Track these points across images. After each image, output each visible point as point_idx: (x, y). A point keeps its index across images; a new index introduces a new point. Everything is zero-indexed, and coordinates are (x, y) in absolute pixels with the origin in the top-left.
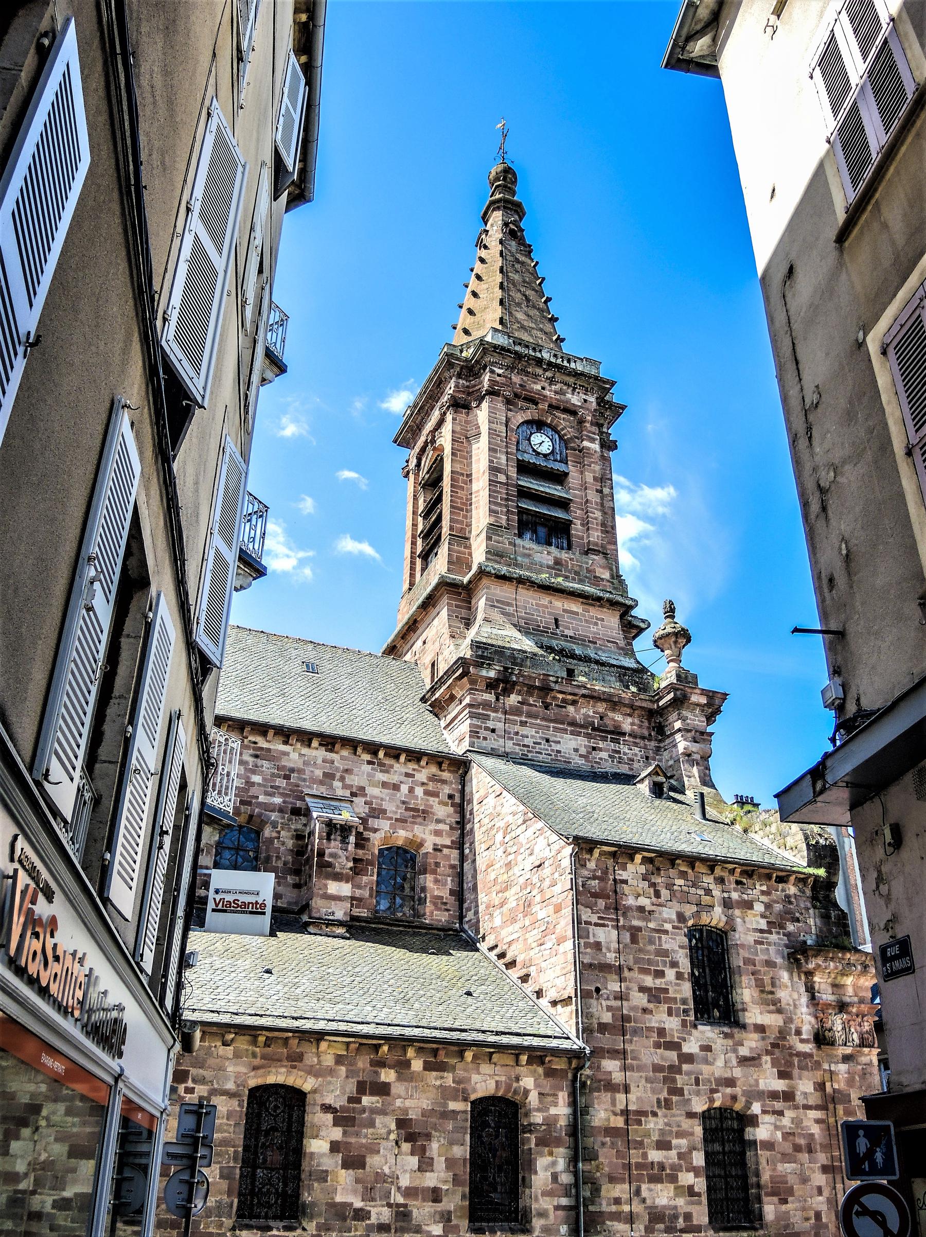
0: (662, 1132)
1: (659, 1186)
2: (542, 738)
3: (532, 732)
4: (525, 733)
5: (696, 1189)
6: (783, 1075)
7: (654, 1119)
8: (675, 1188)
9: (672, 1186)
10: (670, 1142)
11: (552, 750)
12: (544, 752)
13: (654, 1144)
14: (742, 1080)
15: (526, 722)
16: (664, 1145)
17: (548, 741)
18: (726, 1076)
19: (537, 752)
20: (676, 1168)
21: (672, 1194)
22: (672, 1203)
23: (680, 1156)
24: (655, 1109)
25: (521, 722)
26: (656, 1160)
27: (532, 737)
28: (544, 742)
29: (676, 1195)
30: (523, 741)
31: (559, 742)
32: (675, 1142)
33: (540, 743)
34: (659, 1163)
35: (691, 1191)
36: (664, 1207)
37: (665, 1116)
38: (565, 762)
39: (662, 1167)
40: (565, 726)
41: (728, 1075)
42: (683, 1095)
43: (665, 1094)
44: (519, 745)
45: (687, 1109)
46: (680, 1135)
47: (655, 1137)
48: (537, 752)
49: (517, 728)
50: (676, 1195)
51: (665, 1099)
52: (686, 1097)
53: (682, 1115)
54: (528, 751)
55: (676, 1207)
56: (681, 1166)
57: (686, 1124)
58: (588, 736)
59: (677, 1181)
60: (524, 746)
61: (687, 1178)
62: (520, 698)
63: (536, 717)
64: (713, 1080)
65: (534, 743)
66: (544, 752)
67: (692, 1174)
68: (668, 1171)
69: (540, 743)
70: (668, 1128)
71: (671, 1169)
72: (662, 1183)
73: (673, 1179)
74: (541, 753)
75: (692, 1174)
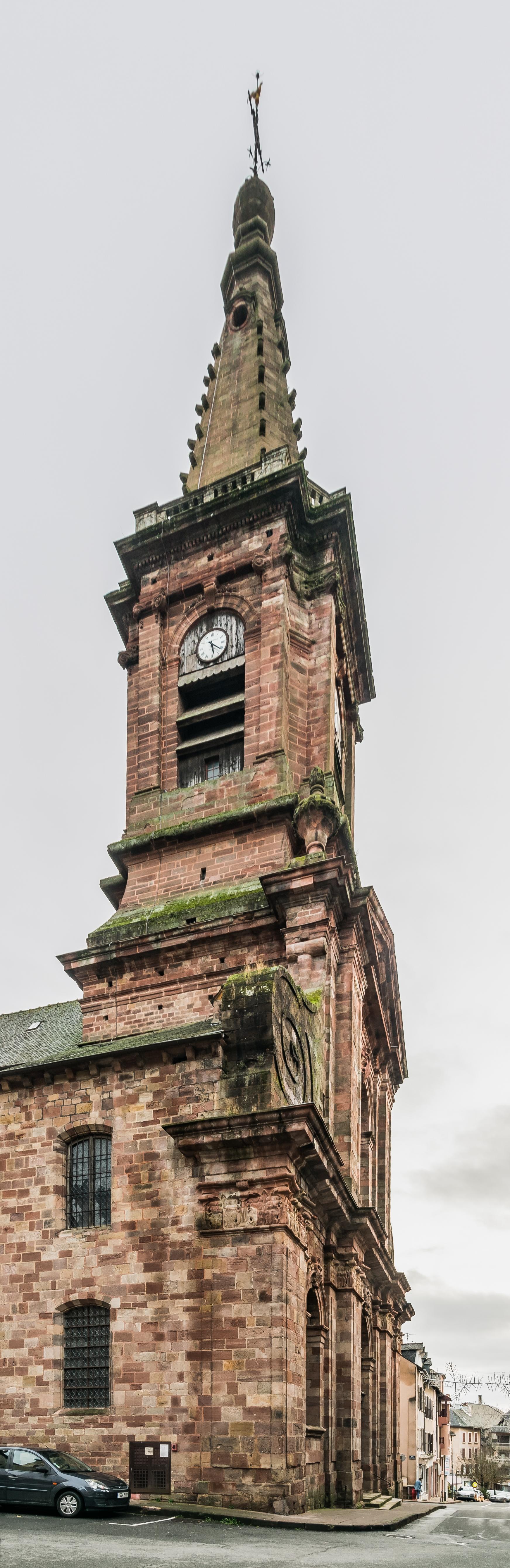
0: (15, 1334)
1: (10, 1378)
2: (153, 1007)
3: (145, 1005)
4: (137, 1008)
5: (44, 1379)
6: (148, 1268)
7: (9, 1322)
8: (24, 1379)
9: (21, 1378)
10: (23, 1341)
11: (165, 1016)
12: (155, 1021)
13: (7, 1344)
14: (102, 1278)
15: (137, 997)
16: (16, 1344)
17: (160, 1007)
18: (85, 1276)
19: (149, 1024)
20: (26, 1363)
21: (21, 1384)
22: (21, 1391)
23: (31, 1352)
24: (11, 1314)
25: (132, 999)
26: (8, 1357)
27: (144, 1009)
28: (157, 1010)
29: (25, 1385)
30: (134, 1017)
31: (172, 1004)
32: (27, 1340)
33: (152, 1013)
34: (10, 1359)
35: (40, 1381)
36: (13, 1395)
37: (20, 1319)
38: (178, 1023)
39: (13, 1362)
40: (179, 986)
41: (87, 1276)
42: (38, 1299)
43: (21, 1301)
44: (130, 1023)
45: (41, 1311)
46: (32, 1334)
47: (9, 1338)
48: (149, 1024)
49: (128, 1007)
50: (25, 1385)
51: (20, 1305)
52: (41, 1301)
53: (36, 1317)
54: (140, 1026)
55: (24, 1395)
56: (31, 1360)
57: (40, 1324)
58: (204, 986)
59: (27, 1374)
60: (135, 1022)
61: (36, 1370)
62: (132, 975)
63: (145, 988)
64: (70, 1282)
65: (146, 1015)
66: (155, 1021)
67: (41, 1367)
68: (18, 1365)
69: (152, 1013)
70: (22, 1329)
71: (22, 1364)
72: (13, 1375)
73: (23, 1371)
74: (152, 1023)
75: (41, 1367)
